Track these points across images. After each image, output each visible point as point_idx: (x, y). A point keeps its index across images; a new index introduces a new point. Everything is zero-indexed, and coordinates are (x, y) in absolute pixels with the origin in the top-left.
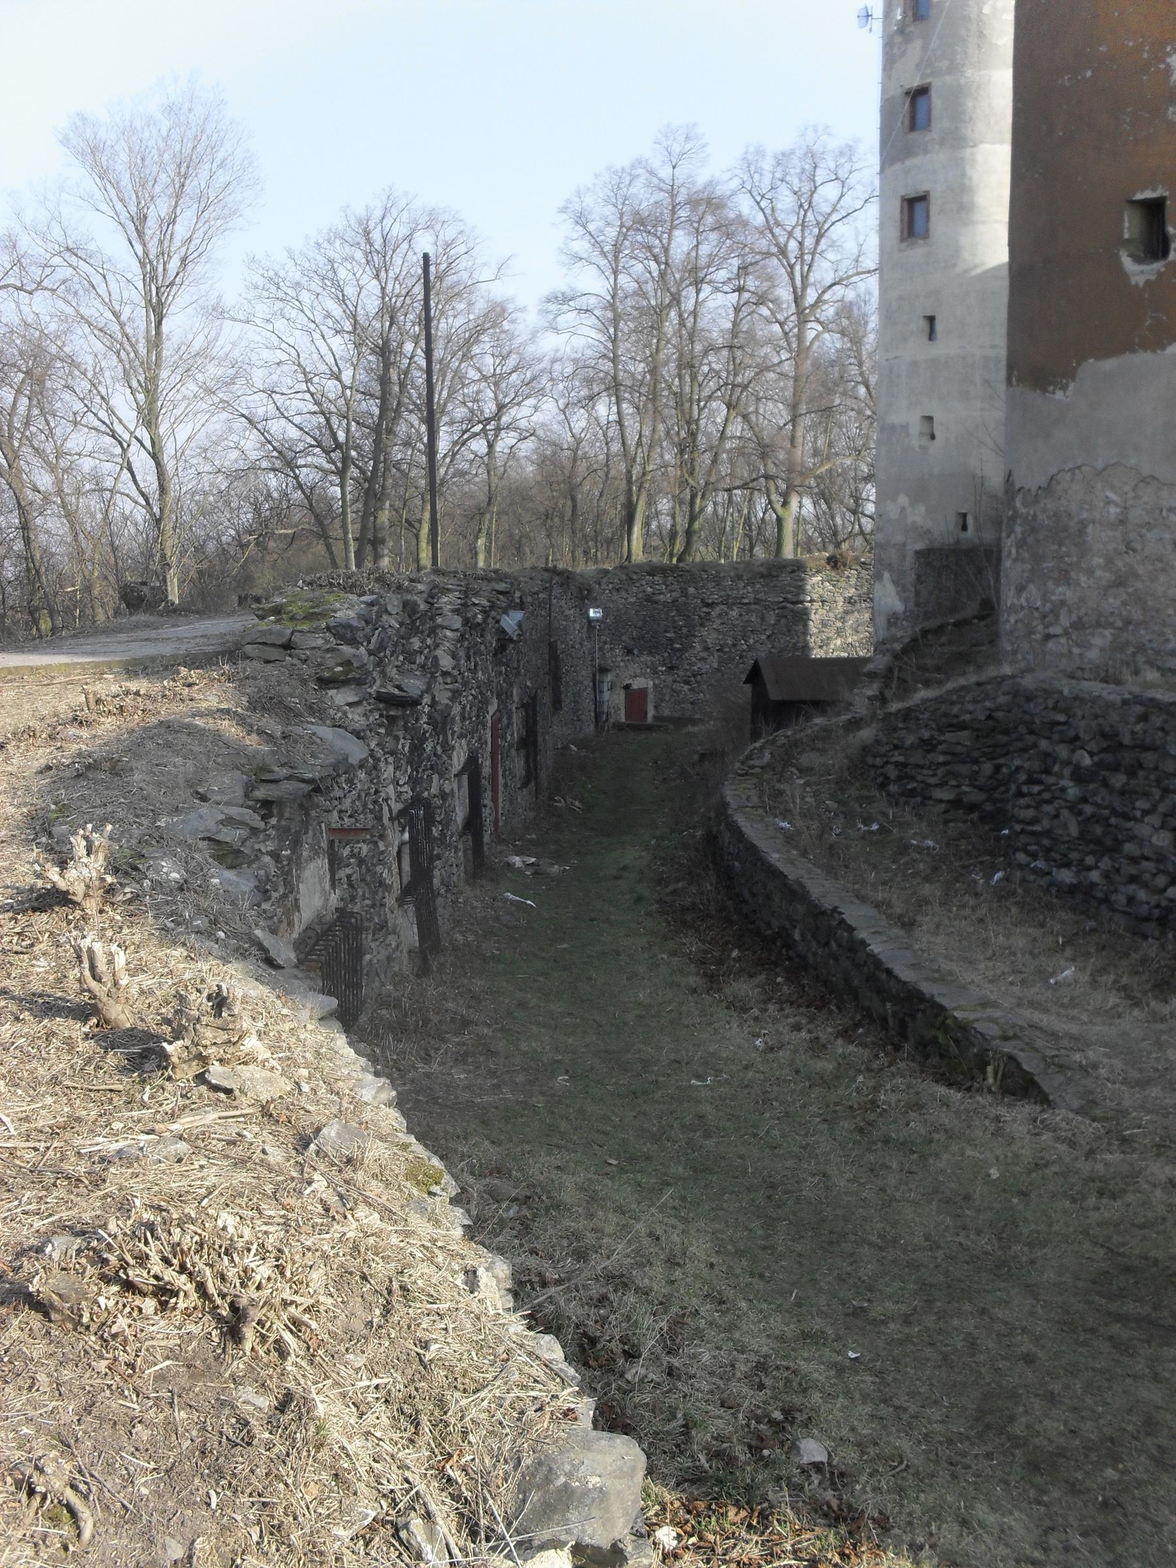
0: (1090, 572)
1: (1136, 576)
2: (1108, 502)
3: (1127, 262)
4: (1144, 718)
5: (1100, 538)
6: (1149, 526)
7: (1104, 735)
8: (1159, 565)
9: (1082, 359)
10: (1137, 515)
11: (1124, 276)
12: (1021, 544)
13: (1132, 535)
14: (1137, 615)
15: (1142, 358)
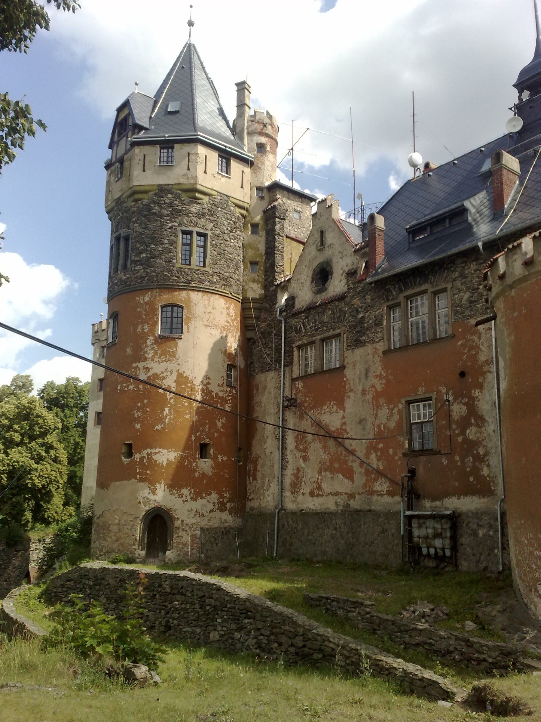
0: (111, 537)
1: (122, 538)
2: (116, 519)
3: (123, 458)
4: (102, 572)
5: (114, 528)
6: (125, 525)
7: (95, 577)
8: (127, 535)
9: (112, 482)
10: (122, 522)
11: (122, 461)
12: (95, 530)
13: (121, 528)
14: (122, 549)
15: (125, 482)
